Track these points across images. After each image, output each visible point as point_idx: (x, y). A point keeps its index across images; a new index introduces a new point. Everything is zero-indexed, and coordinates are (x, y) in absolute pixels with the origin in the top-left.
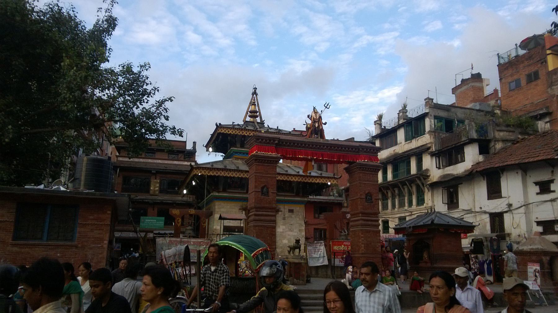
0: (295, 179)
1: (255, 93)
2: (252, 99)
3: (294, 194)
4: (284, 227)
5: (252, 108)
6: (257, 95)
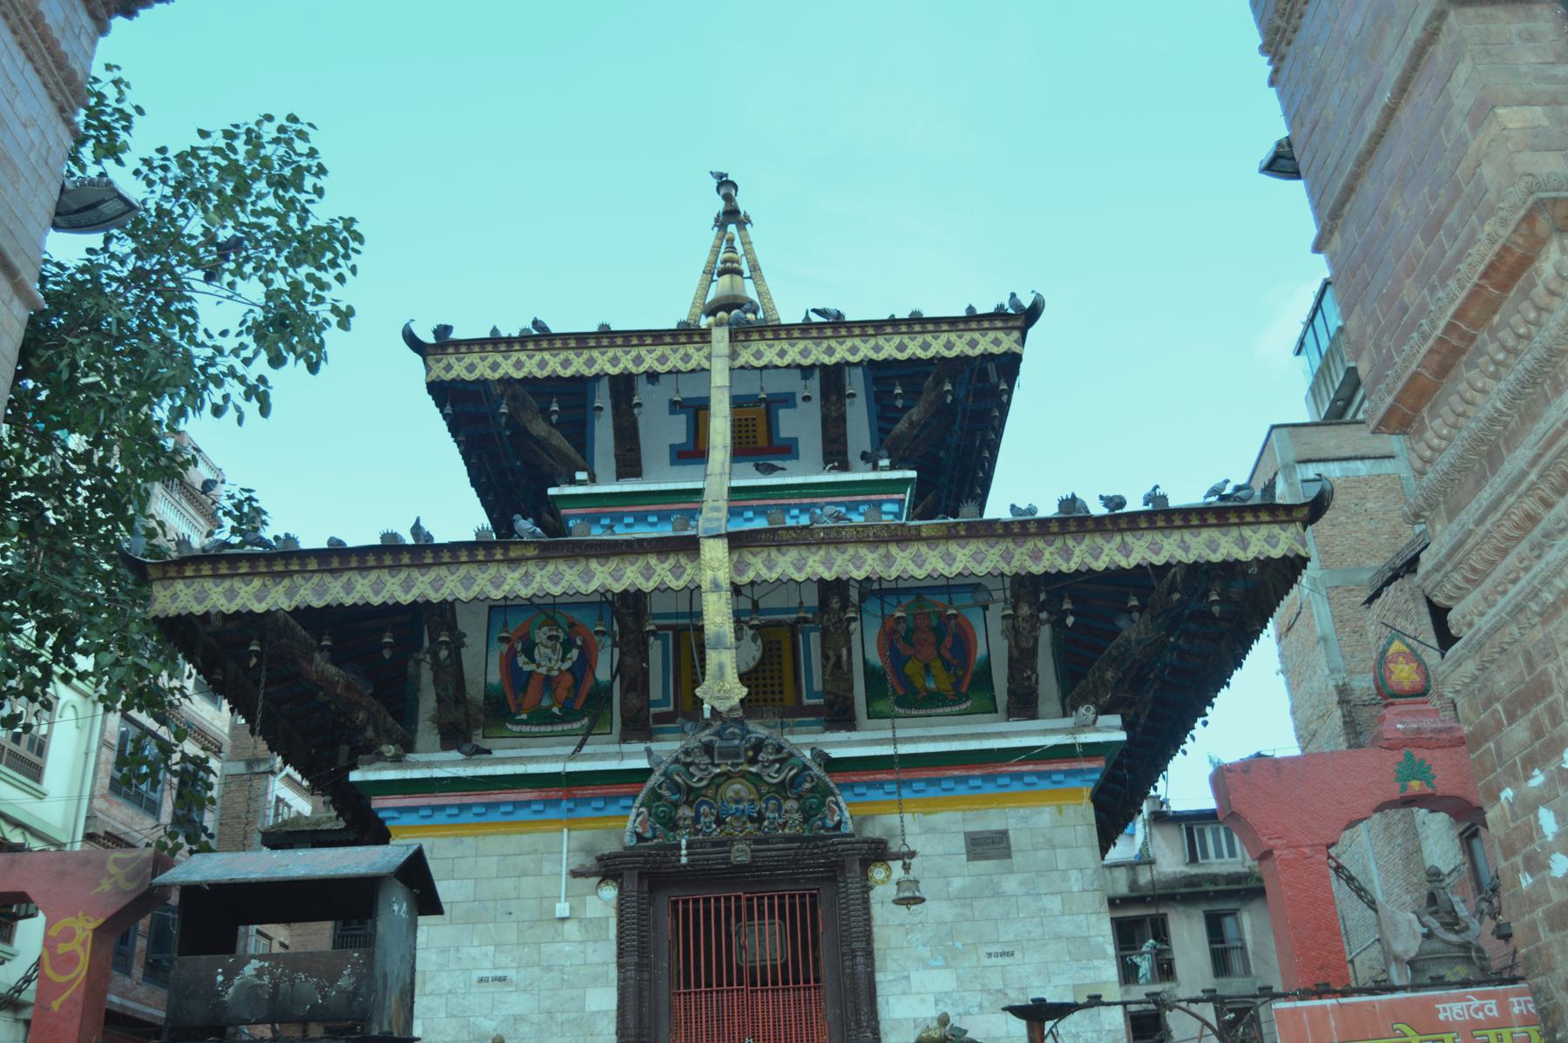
1: (731, 215)
2: (715, 251)
4: (941, 980)
5: (720, 287)
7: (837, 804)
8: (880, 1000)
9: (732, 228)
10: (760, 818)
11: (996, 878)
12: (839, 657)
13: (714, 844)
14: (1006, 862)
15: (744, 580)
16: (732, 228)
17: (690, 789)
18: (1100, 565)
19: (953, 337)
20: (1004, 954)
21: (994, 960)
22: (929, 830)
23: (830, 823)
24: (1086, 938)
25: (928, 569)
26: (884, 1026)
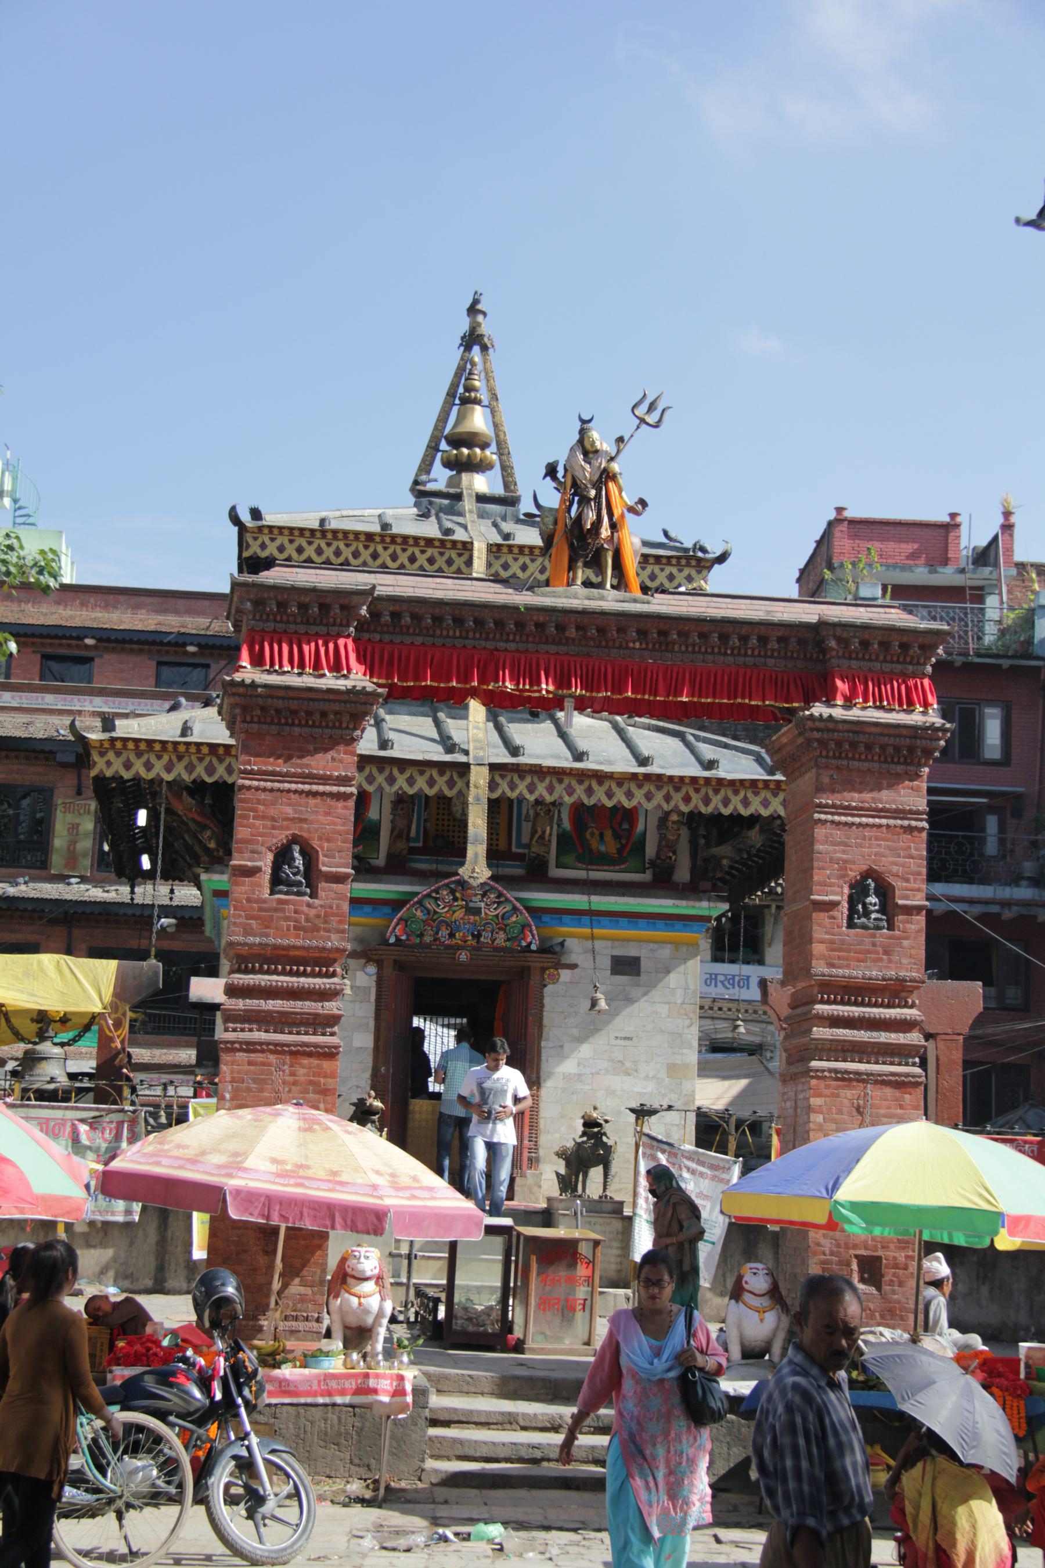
0: (629, 795)
2: (460, 370)
3: (647, 877)
6: (484, 348)
7: (531, 931)
8: (543, 1058)
9: (476, 349)
10: (479, 936)
11: (627, 988)
12: (544, 832)
13: (449, 947)
14: (636, 978)
15: (495, 796)
17: (435, 912)
18: (726, 812)
19: (656, 569)
20: (625, 1038)
21: (619, 1042)
23: (524, 944)
24: (680, 1035)
25: (614, 801)
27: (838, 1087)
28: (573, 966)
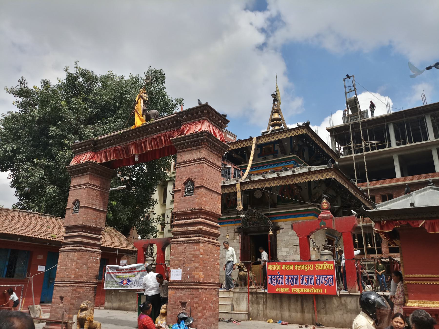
4: (287, 249)
16: (276, 102)
19: (294, 132)
22: (286, 224)
26: (278, 257)
27: (179, 246)
28: (283, 229)
